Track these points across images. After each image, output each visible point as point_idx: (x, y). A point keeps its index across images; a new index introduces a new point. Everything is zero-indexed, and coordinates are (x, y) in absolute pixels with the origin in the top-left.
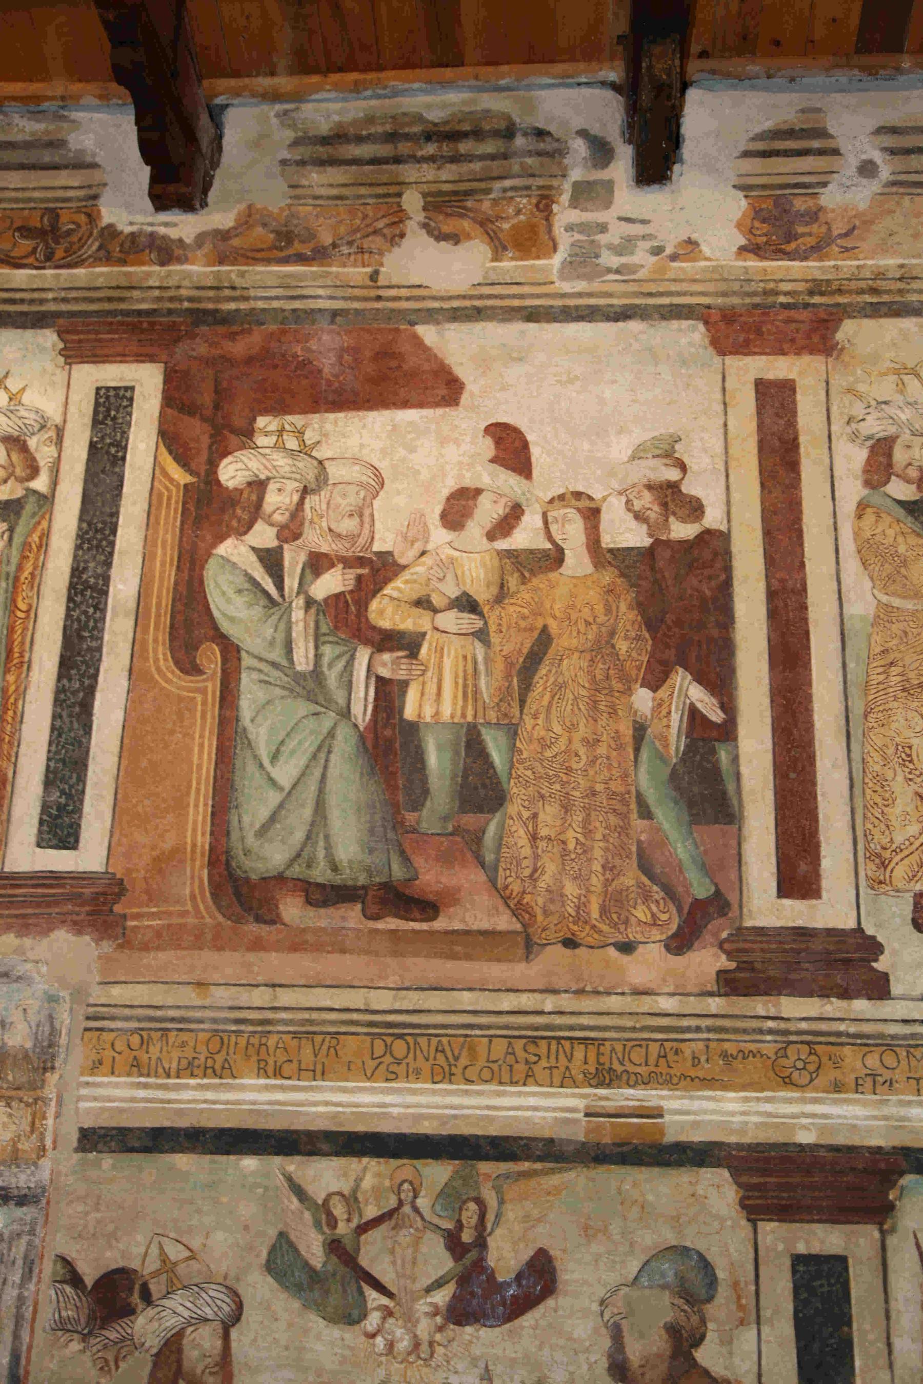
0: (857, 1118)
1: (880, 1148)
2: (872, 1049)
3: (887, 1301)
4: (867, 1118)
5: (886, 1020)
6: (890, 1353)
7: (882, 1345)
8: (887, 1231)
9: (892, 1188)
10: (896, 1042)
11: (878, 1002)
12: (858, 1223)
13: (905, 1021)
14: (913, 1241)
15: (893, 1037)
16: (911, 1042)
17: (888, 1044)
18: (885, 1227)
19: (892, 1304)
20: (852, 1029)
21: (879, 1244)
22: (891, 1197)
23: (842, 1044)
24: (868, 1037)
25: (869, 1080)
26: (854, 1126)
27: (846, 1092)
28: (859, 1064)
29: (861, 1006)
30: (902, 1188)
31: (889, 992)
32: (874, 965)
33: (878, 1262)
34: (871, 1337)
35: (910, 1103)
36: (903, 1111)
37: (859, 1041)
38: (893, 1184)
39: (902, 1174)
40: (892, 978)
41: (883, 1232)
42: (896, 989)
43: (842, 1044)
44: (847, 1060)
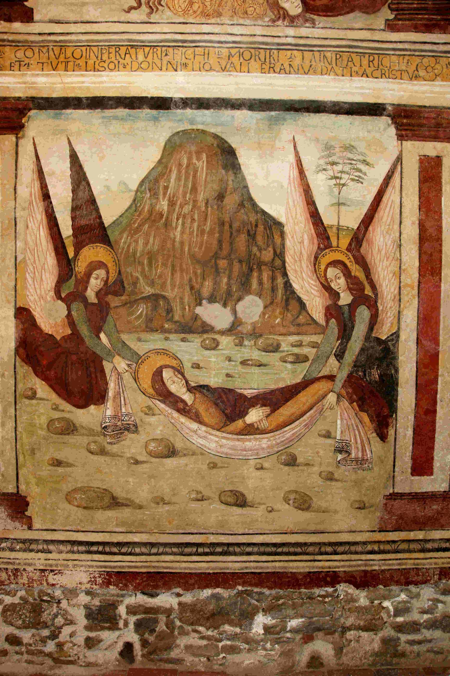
0: (9, 83)
1: (20, 98)
2: (20, 48)
3: (16, 170)
4: (15, 83)
5: (30, 34)
6: (15, 193)
7: (12, 190)
8: (19, 138)
9: (24, 117)
10: (33, 45)
11: (27, 24)
12: (5, 134)
13: (40, 34)
14: (32, 141)
15: (32, 42)
16: (42, 44)
17: (29, 45)
18: (19, 135)
19: (19, 171)
20: (11, 38)
21: (15, 144)
22: (23, 121)
23: (4, 46)
24: (19, 42)
25: (17, 63)
26: (8, 87)
27: (5, 70)
28: (13, 56)
29: (17, 26)
30: (29, 118)
31: (33, 19)
32: (26, 3)
33: (14, 152)
34: (7, 186)
35: (38, 75)
36: (34, 79)
37: (14, 44)
38: (25, 115)
39: (30, 110)
40: (35, 11)
41: (17, 138)
42: (36, 17)
43: (4, 46)
44: (6, 54)
